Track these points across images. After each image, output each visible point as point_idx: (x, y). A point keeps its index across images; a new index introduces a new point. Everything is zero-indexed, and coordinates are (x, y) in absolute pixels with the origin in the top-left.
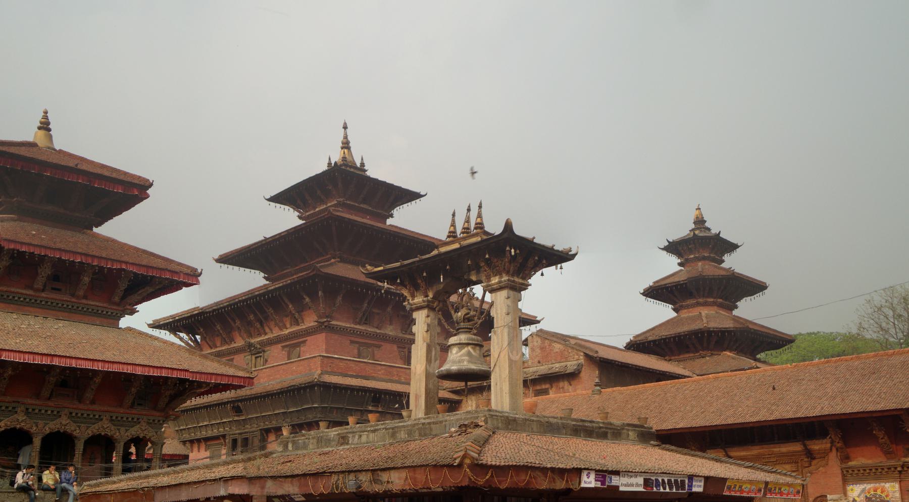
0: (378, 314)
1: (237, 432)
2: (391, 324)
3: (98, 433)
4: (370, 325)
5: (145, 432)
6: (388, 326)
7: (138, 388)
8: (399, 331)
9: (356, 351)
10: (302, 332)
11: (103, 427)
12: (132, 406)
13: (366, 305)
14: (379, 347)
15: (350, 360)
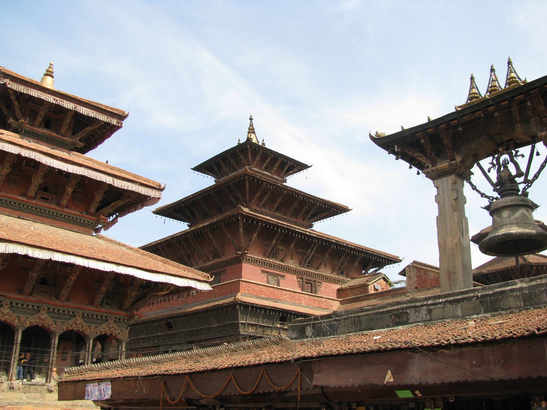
0: (282, 250)
1: (169, 343)
2: (291, 259)
3: (71, 328)
4: (276, 258)
5: (112, 330)
6: (289, 260)
7: (108, 288)
8: (298, 265)
9: (266, 279)
10: (223, 263)
11: (76, 323)
12: (102, 305)
13: (275, 241)
14: (283, 276)
15: (263, 285)
